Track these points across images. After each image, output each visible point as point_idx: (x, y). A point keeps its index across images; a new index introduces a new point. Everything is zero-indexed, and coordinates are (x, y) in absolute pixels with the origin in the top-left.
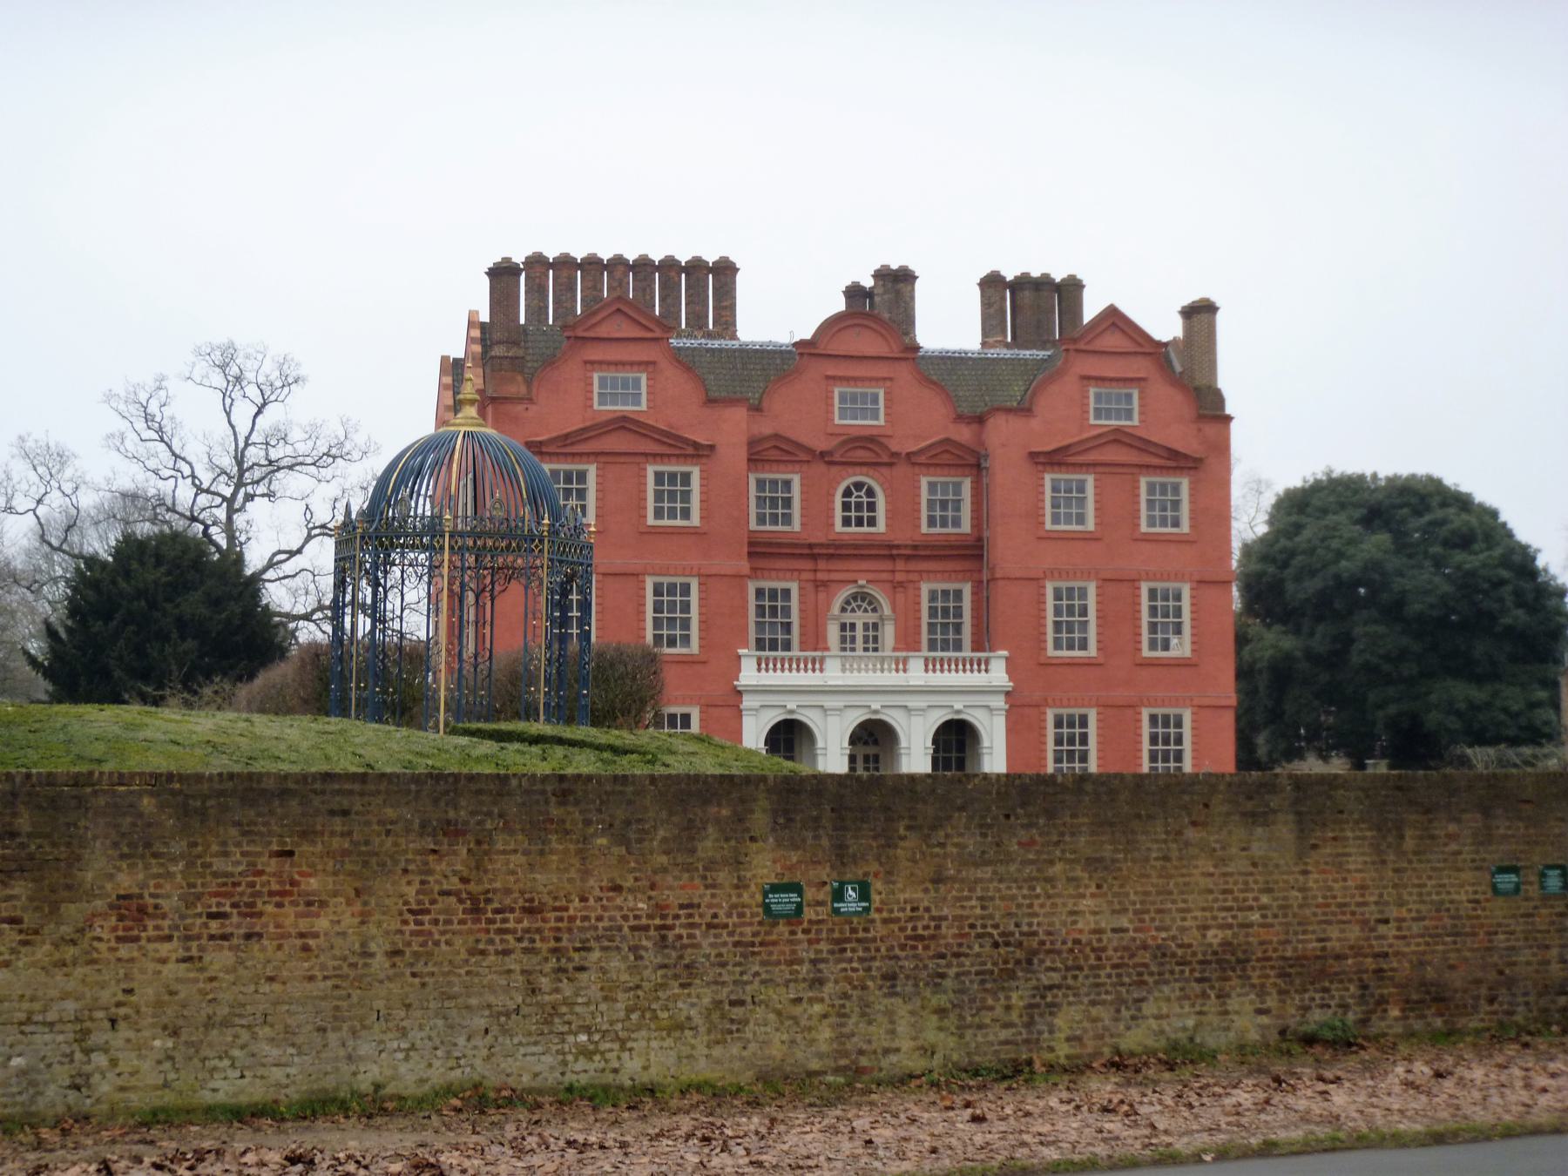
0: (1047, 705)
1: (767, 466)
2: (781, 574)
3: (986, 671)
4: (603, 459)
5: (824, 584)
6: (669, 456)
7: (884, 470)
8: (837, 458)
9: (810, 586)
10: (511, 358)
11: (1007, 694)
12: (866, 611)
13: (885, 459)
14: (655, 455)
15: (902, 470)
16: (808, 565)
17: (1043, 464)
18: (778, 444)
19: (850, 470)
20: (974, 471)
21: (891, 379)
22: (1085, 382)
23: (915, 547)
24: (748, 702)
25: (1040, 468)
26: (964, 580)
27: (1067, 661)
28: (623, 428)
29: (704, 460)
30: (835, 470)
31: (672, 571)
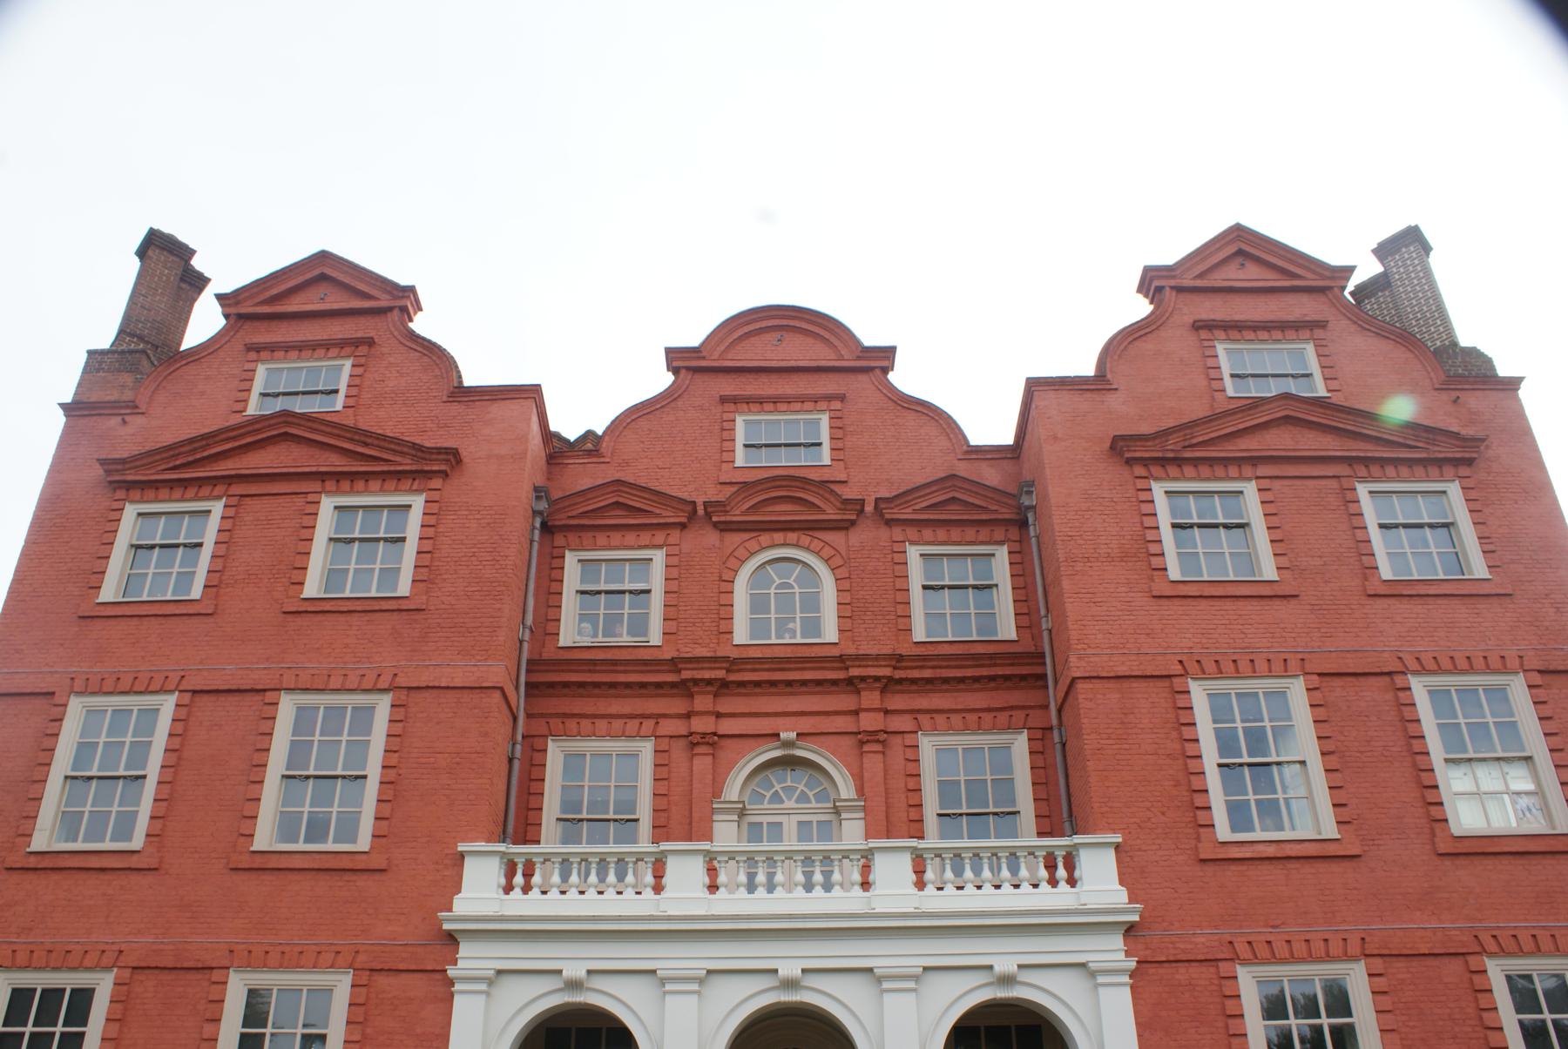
0: (1235, 958)
1: (601, 538)
2: (617, 724)
3: (1072, 882)
4: (238, 489)
5: (711, 742)
6: (367, 476)
7: (830, 537)
8: (736, 516)
9: (678, 750)
10: (123, 352)
11: (1130, 930)
12: (803, 798)
13: (831, 513)
14: (338, 476)
15: (864, 536)
16: (678, 705)
17: (1145, 462)
18: (621, 500)
19: (765, 538)
20: (1014, 533)
21: (842, 398)
22: (1204, 334)
23: (898, 660)
24: (472, 959)
25: (1139, 470)
26: (1010, 728)
27: (1270, 851)
28: (286, 436)
29: (436, 483)
30: (734, 539)
31: (335, 682)
